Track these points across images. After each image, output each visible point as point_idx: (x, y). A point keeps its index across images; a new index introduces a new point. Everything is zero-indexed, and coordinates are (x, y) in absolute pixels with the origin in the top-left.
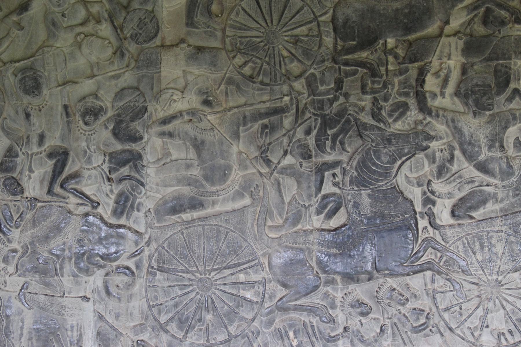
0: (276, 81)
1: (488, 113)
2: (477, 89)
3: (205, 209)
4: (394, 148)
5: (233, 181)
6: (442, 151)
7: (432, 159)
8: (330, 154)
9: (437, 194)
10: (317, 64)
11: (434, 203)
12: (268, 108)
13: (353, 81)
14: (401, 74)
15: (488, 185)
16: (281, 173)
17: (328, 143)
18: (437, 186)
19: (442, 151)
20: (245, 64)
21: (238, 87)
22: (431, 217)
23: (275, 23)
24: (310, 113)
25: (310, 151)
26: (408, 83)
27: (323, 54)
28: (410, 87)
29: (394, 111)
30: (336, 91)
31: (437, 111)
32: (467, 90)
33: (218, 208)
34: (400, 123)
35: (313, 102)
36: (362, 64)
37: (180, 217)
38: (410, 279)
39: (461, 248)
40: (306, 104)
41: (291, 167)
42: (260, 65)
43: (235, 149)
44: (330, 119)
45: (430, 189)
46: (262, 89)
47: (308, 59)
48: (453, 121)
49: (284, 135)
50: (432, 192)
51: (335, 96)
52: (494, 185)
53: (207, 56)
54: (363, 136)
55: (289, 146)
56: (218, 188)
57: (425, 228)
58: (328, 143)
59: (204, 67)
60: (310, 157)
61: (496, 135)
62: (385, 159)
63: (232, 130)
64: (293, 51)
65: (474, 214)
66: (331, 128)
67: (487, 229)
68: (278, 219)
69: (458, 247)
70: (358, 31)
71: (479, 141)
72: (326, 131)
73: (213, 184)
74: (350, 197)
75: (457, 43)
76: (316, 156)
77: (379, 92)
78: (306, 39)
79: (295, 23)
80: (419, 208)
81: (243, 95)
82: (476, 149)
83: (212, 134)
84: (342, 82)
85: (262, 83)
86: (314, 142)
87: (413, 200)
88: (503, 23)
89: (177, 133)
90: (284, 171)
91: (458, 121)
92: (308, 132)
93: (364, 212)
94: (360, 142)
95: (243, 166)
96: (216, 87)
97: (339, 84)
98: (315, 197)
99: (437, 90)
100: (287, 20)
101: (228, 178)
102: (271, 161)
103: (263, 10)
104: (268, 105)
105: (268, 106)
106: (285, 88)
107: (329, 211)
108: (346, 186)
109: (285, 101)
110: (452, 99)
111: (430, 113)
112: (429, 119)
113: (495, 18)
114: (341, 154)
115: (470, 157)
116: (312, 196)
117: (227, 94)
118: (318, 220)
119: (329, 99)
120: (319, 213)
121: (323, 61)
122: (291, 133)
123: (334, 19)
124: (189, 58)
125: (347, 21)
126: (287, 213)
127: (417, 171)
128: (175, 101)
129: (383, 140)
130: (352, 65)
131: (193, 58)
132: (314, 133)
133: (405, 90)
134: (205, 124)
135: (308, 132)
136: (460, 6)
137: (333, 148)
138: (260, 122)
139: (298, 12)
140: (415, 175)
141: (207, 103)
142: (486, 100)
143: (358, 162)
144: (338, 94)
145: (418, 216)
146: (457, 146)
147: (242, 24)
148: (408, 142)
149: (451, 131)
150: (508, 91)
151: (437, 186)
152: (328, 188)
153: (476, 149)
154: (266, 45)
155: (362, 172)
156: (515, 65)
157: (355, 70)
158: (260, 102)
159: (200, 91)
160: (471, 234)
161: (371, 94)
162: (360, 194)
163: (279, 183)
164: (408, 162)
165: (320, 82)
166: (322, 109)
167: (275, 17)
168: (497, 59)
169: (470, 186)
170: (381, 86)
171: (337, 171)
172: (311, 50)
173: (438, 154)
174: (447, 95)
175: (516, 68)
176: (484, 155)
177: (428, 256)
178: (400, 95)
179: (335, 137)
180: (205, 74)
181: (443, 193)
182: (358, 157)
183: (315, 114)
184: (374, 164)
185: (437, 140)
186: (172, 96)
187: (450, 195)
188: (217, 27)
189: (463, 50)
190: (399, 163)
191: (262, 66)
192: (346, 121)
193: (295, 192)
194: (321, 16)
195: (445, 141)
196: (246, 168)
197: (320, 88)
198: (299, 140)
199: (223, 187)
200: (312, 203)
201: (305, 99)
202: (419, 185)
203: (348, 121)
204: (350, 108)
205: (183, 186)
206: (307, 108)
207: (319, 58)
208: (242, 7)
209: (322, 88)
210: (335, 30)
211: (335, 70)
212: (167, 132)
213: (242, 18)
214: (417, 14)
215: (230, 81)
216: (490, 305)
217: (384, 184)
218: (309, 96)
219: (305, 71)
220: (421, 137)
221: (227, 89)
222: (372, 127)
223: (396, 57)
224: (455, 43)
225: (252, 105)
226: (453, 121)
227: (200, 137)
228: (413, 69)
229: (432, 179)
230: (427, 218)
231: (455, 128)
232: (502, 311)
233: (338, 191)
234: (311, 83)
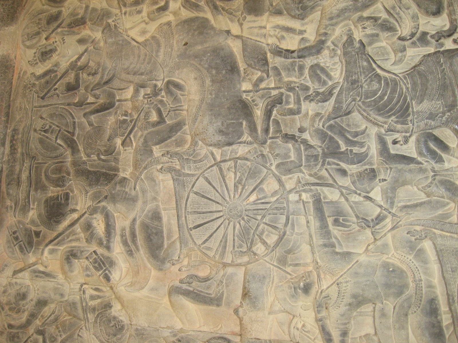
0: (284, 208)
3: (437, 297)
4: (363, 76)
5: (402, 262)
7: (374, 37)
8: (369, 148)
9: (414, 31)
10: (266, 162)
11: (425, 34)
12: (314, 218)
13: (286, 125)
14: (279, 74)
16: (392, 203)
17: (356, 150)
18: (405, 30)
19: (364, 28)
20: (264, 243)
21: (289, 252)
22: (440, 36)
23: (220, 208)
24: (320, 170)
25: (366, 170)
26: (289, 67)
27: (255, 156)
28: (293, 64)
29: (319, 79)
30: (297, 141)
31: (320, 35)
32: (298, 8)
33: (436, 280)
34: (332, 74)
35: (308, 167)
36: (268, 114)
37: (447, 327)
40: (310, 175)
41: (384, 192)
42: (266, 226)
43: (363, 259)
44: (328, 148)
45: (408, 38)
46: (293, 225)
47: (260, 172)
48: (331, 19)
49: (347, 200)
50: (413, 35)
51: (302, 143)
53: (253, 286)
54: (348, 110)
55: (360, 195)
56: (410, 280)
58: (356, 150)
59: (265, 289)
60: (373, 170)
62: (375, 86)
63: (340, 261)
64: (251, 188)
66: (338, 147)
68: (449, 209)
70: (232, 119)
72: (342, 153)
73: (405, 286)
74: (422, 124)
75: (249, 22)
76: (371, 164)
77: (298, 96)
78: (238, 174)
79: (221, 186)
80: (432, 50)
81: (298, 247)
83: (345, 285)
84: (286, 134)
85: (286, 225)
86: (355, 166)
87: (422, 56)
89: (342, 327)
90: (391, 200)
91: (331, 13)
92: (343, 173)
93: (440, 108)
94: (355, 115)
95: (384, 249)
96: (289, 277)
97: (289, 138)
98: (422, 164)
99: (298, 38)
100: (217, 194)
101: (398, 268)
102: (379, 215)
103: (206, 221)
104: (311, 218)
105: (312, 217)
106: (293, 197)
107: (438, 148)
108: (409, 128)
109: (307, 198)
110: (306, 24)
111: (323, 42)
112: (329, 43)
114: (368, 135)
116: (421, 168)
117: (297, 265)
118: (449, 161)
119: (306, 150)
120: (440, 160)
121: (263, 156)
122: (344, 191)
123: (218, 145)
124: (255, 307)
125: (221, 132)
126: (443, 197)
127: (388, 54)
128: (304, 326)
129: (353, 89)
130: (268, 125)
131: (254, 302)
132: (344, 165)
133: (296, 69)
134: (333, 292)
135: (343, 173)
136: (213, 22)
137: (362, 145)
138: (331, 227)
139: (210, 183)
141: (307, 289)
143: (380, 115)
144: (299, 140)
145: (442, 49)
146: (358, 14)
147: (220, 245)
148: (355, 62)
149: (342, 21)
152: (410, 149)
154: (243, 219)
155: (391, 109)
157: (273, 122)
158: (308, 227)
159: (293, 296)
161: (301, 104)
162: (418, 112)
163: (405, 207)
165: (286, 159)
166: (316, 157)
167: (214, 207)
170: (291, 94)
171: (389, 140)
172: (250, 169)
173: (369, 31)
174: (303, 29)
178: (301, 74)
179: (349, 142)
180: (273, 288)
181: (413, 24)
182: (374, 115)
183: (323, 164)
184: (381, 98)
185: (352, 34)
186: (298, 329)
187: (415, 17)
188: (222, 273)
189: (256, 15)
190: (379, 71)
191: (266, 224)
192: (331, 131)
193: (415, 188)
194: (215, 159)
195: (353, 27)
196: (385, 246)
197: (293, 159)
198: (353, 183)
199: (409, 274)
200: (429, 167)
201: (305, 175)
202: (403, 50)
203: (331, 127)
204: (316, 126)
205: (407, 322)
206: (316, 174)
207: (260, 160)
208: (202, 244)
209: (293, 156)
210: (230, 144)
211: (272, 143)
212: (341, 338)
213: (214, 244)
214: (218, 61)
215: (283, 261)
217: (405, 86)
218: (301, 171)
219: (274, 175)
220: (350, 49)
221: (291, 265)
222: (338, 101)
223: (261, 80)
224: (249, 23)
225: (311, 236)
226: (331, 19)
227: (348, 299)
228: (274, 61)
229: (397, 36)
230: (442, 40)
231: (338, 16)
233: (413, 139)
234: (286, 168)
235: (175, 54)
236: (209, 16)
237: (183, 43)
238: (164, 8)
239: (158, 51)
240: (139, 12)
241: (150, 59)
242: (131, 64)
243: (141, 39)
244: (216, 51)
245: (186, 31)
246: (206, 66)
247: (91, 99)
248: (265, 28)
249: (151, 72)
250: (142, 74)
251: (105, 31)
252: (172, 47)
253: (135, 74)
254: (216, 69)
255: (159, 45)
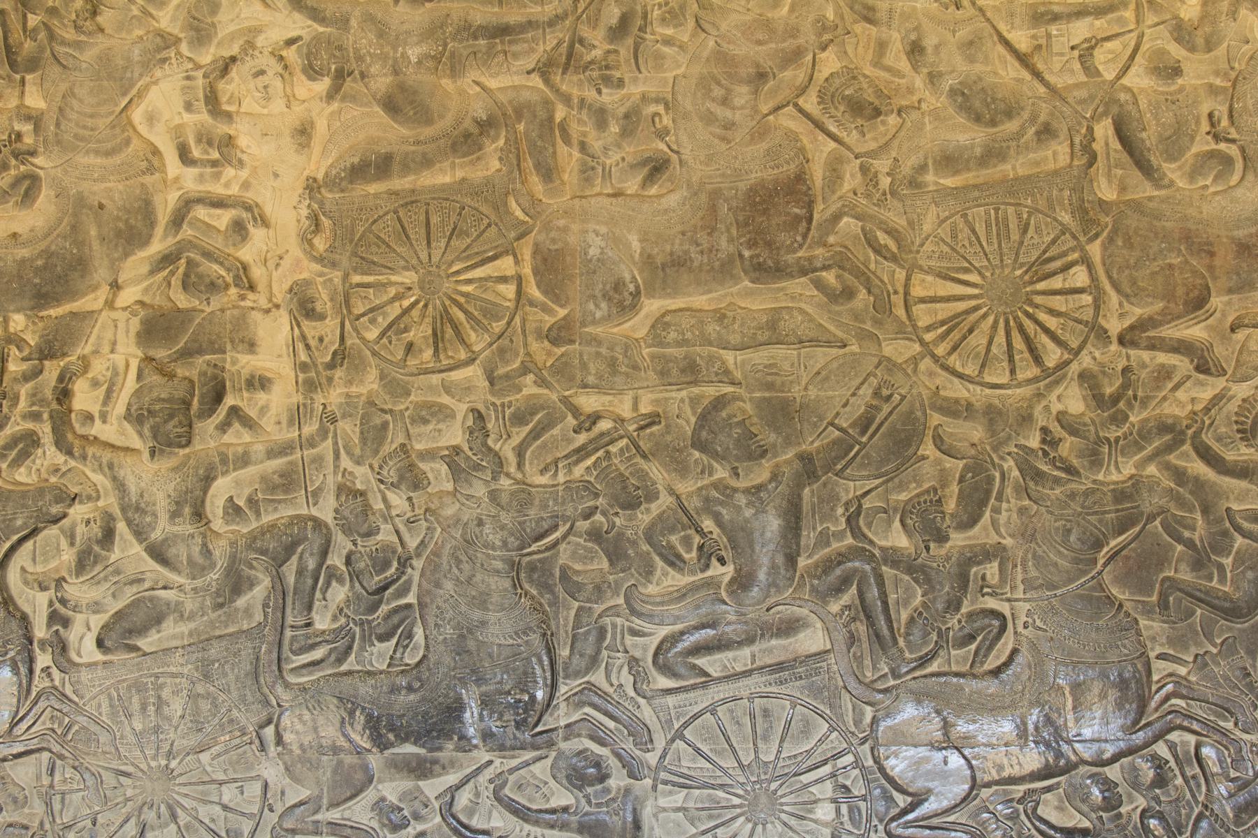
1: (182, 452)
2: (157, 407)
6: (88, 522)
11: (66, 622)
15: (165, 588)
18: (76, 590)
22: (61, 647)
26: (39, 396)
34: (22, 470)
38: (11, 768)
39: (105, 708)
50: (63, 601)
52: (178, 588)
57: (46, 670)
61: (186, 493)
65: (142, 643)
67: (156, 671)
69: (100, 706)
71: (154, 505)
82: (148, 519)
88: (214, 287)
91: (120, 467)
112: (73, 463)
113: (200, 276)
115: (139, 534)
127: (46, 561)
133: (34, 408)
140: (40, 569)
142: (175, 427)
146: (117, 512)
148: (24, 506)
150: (222, 411)
151: (76, 590)
153: (148, 519)
156: (234, 363)
160: (124, 681)
164: (29, 545)
168: (200, 351)
169: (135, 589)
173: (80, 530)
175: (233, 369)
176: (161, 529)
177: (44, 723)
178: (24, 417)
181: (84, 603)
185: (81, 502)
187: (96, 607)
189: (138, 334)
202: (43, 588)
216: (149, 816)
226: (111, 466)
232: (173, 827)
235: (85, 186)
236: (157, 246)
237: (103, 201)
238: (185, 156)
239: (97, 152)
240: (188, 107)
241: (82, 139)
242: (81, 101)
243: (137, 115)
244: (81, 265)
245: (128, 206)
246: (53, 248)
247: (33, 20)
248: (112, 351)
249: (59, 142)
250: (58, 125)
251: (158, 40)
252: (102, 179)
253: (61, 109)
254: (45, 267)
255: (108, 154)
